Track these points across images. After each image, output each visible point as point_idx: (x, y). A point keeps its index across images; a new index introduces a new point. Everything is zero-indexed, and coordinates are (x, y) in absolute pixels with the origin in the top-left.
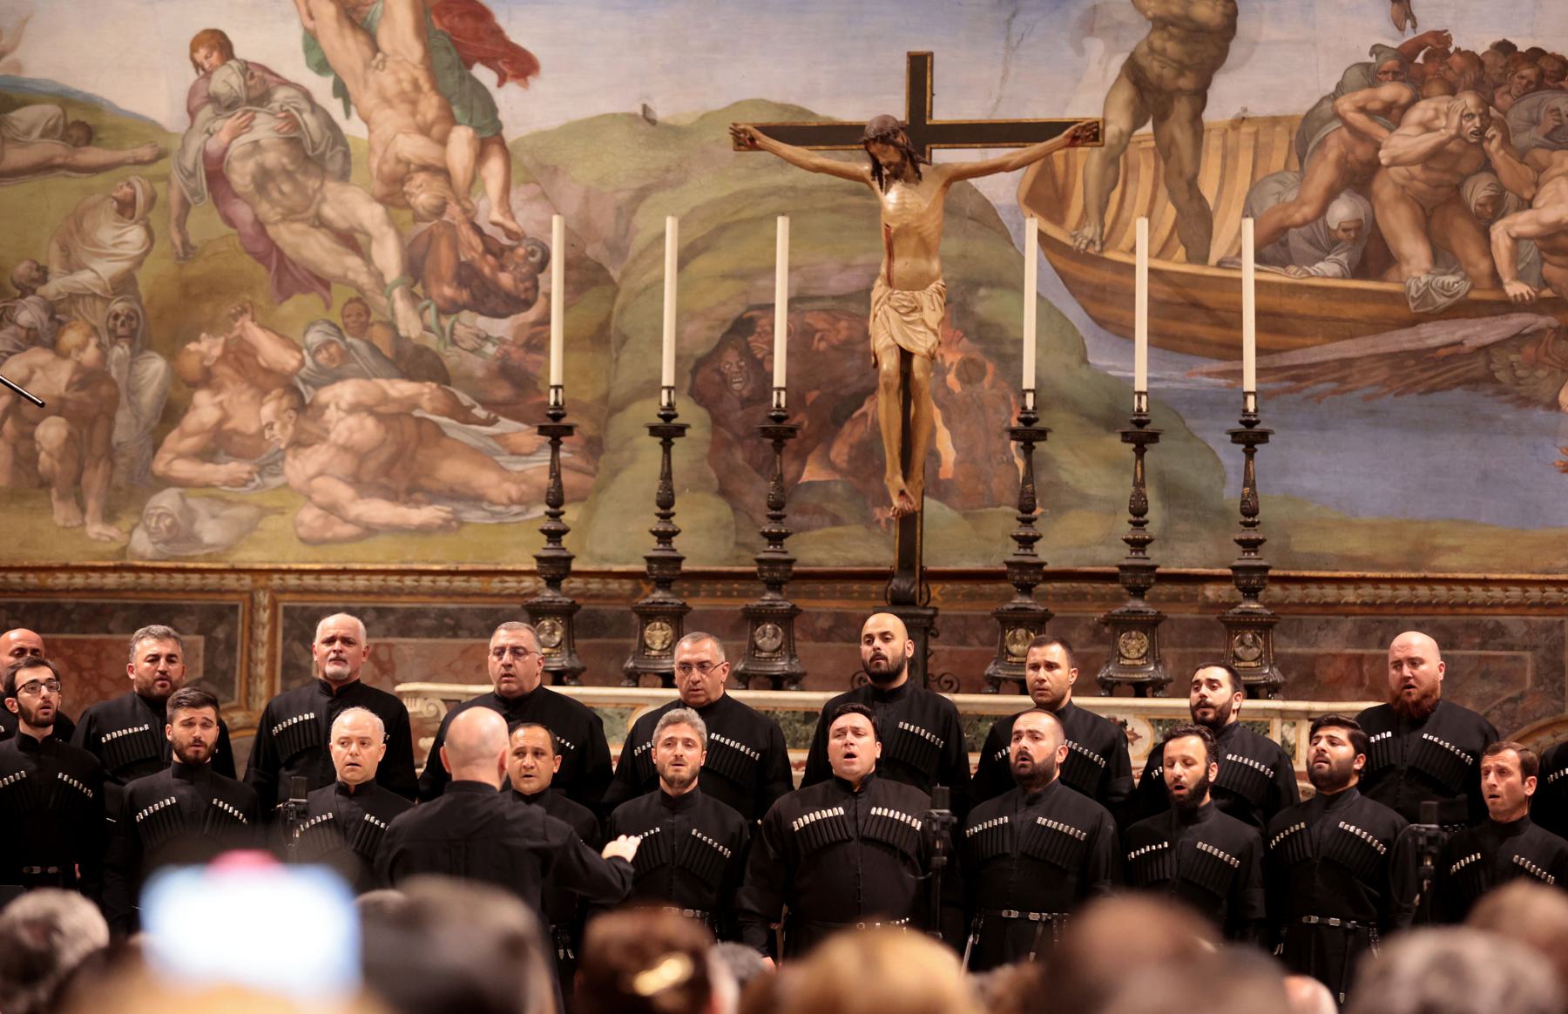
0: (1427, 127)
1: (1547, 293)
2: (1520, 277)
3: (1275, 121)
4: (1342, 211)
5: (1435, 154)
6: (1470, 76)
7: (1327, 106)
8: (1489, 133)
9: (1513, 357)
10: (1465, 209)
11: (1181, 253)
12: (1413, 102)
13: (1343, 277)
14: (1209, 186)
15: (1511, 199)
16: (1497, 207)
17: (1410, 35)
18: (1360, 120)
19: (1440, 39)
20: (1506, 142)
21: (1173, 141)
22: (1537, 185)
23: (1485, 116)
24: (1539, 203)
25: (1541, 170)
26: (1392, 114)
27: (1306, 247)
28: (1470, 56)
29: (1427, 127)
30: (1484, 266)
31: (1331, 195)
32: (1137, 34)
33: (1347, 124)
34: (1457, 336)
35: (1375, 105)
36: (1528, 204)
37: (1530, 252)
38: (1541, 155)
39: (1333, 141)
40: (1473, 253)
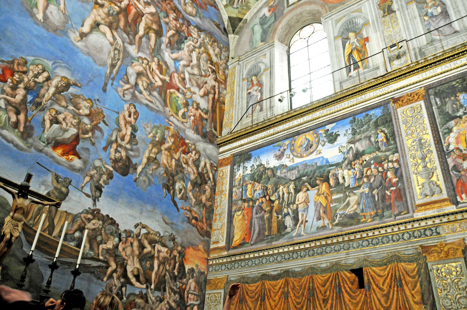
0: (94, 224)
1: (105, 260)
2: (102, 256)
3: (70, 214)
4: (77, 234)
5: (94, 229)
6: (102, 218)
7: (79, 215)
8: (103, 229)
9: (98, 270)
10: (97, 240)
11: (47, 232)
12: (92, 219)
13: (74, 246)
14: (56, 221)
15: (103, 242)
16: (101, 242)
17: (95, 208)
18: (84, 219)
19: (99, 211)
20: (105, 231)
21: (52, 210)
22: (108, 241)
23: (103, 226)
24: (107, 243)
25: (109, 238)
26: (89, 220)
27: (70, 239)
28: (103, 215)
29: (94, 224)
30: (97, 252)
31: (76, 231)
32: (51, 189)
33: (82, 219)
34: (90, 263)
35: (87, 218)
36: (106, 243)
37: (105, 252)
38: (109, 235)
39: (79, 221)
40: (96, 249)
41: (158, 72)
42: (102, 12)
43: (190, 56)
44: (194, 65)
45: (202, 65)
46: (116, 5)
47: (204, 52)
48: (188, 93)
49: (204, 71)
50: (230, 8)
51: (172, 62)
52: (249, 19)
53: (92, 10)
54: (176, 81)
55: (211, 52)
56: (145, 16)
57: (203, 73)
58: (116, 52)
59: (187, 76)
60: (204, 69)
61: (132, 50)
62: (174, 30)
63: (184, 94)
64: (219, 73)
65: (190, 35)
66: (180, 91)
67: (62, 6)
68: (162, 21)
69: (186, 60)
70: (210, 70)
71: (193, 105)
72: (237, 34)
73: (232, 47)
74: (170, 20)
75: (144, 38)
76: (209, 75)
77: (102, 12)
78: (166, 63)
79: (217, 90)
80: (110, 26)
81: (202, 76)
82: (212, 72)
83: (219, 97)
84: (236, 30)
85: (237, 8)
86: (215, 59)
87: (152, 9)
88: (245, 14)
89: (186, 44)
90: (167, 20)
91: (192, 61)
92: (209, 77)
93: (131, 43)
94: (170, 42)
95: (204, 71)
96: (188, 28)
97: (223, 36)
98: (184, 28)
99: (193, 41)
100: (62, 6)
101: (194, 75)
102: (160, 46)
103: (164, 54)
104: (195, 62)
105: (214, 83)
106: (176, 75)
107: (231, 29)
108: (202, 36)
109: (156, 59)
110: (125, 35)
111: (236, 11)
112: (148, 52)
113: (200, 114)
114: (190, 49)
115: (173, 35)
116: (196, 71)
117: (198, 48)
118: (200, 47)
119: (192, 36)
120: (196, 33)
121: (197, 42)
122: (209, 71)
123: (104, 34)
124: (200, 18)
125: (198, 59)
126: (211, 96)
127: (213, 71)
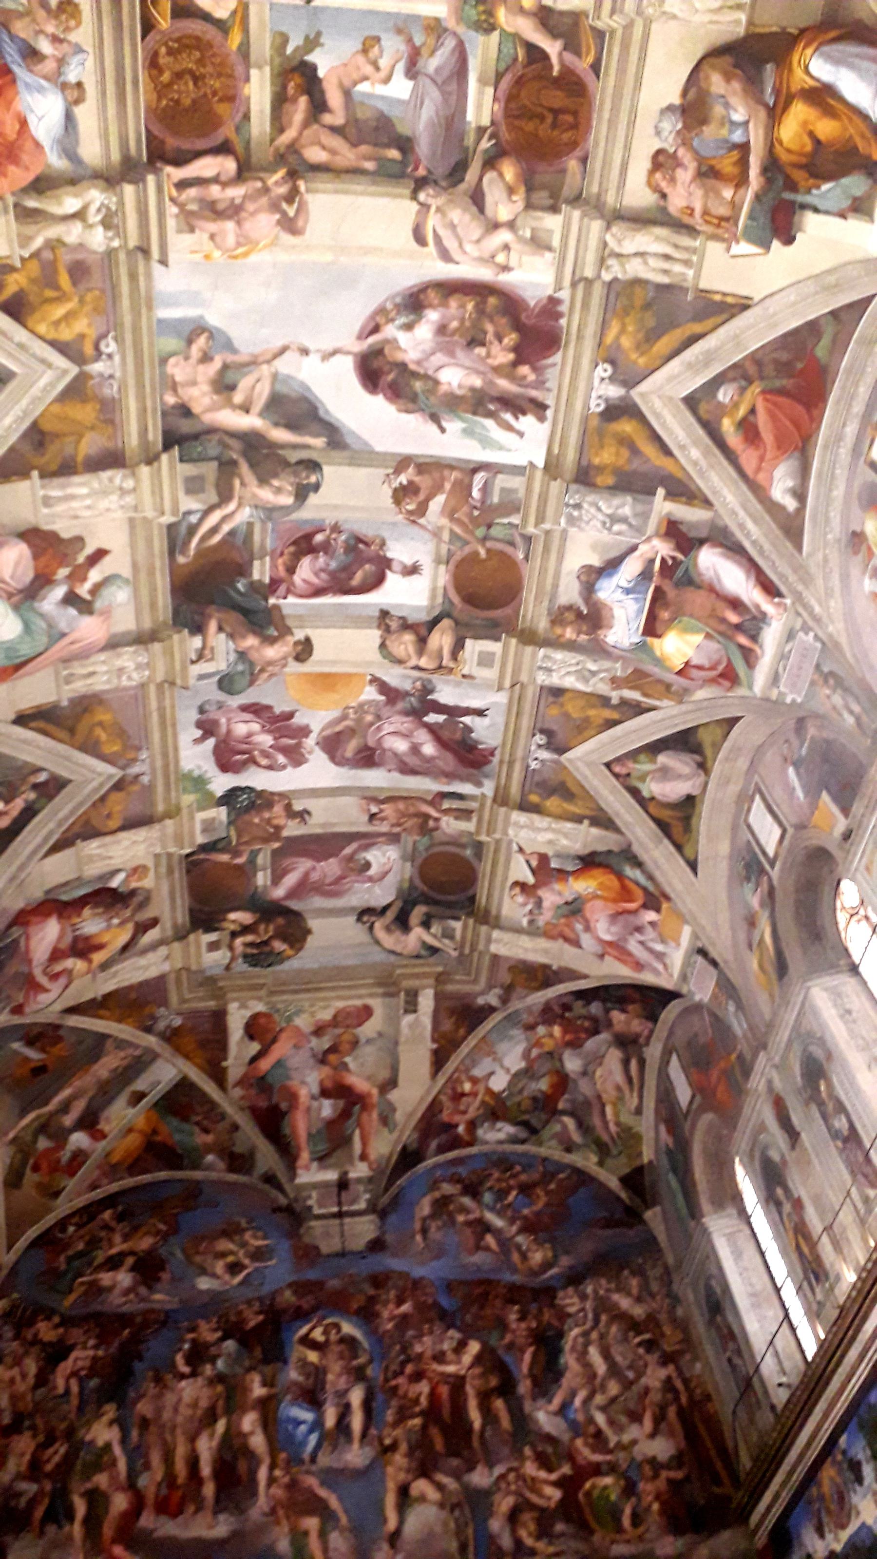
41: (543, 1474)
42: (399, 1459)
43: (587, 1365)
44: (604, 1380)
45: (619, 1359)
46: (413, 1417)
47: (609, 1324)
48: (621, 1455)
49: (630, 1367)
50: (609, 1162)
51: (560, 1422)
52: (652, 1157)
53: (384, 1473)
54: (587, 1454)
55: (624, 1303)
56: (468, 1380)
57: (631, 1375)
58: (457, 1513)
59: (600, 1419)
60: (626, 1363)
61: (480, 1478)
62: (531, 1345)
63: (612, 1469)
64: (663, 1335)
65: (563, 1316)
66: (604, 1468)
67: (344, 1520)
68: (500, 1352)
69: (583, 1386)
70: (641, 1351)
71: (643, 1477)
72: (654, 1204)
73: (662, 1237)
74: (514, 1331)
75: (488, 1428)
76: (646, 1366)
77: (399, 1459)
78: (550, 1439)
79: (679, 1384)
80: (424, 1470)
81: (632, 1383)
82: (648, 1351)
83: (691, 1397)
84: (648, 1197)
85: (620, 1153)
86: (638, 1311)
87: (474, 1347)
88: (640, 1154)
89: (567, 1347)
90: (508, 1338)
91: (594, 1375)
92: (649, 1371)
93: (471, 1468)
94: (536, 1382)
95: (630, 1367)
96: (552, 1305)
97: (631, 1233)
98: (547, 1315)
99: (577, 1325)
100: (344, 1520)
101: (613, 1400)
102: (521, 1410)
103: (536, 1422)
104: (600, 1367)
105: (663, 1373)
106: (579, 1442)
107: (638, 1201)
108: (589, 1290)
109: (527, 1451)
110: (455, 1462)
111: (623, 1159)
112: (506, 1451)
113: (670, 1481)
114: (579, 1347)
115: (535, 1355)
116: (614, 1388)
117: (593, 1328)
118: (597, 1321)
119: (569, 1315)
120: (576, 1300)
121: (585, 1316)
122: (641, 1357)
123: (422, 1499)
124: (567, 1253)
125: (606, 1355)
126: (672, 1412)
127: (650, 1346)
